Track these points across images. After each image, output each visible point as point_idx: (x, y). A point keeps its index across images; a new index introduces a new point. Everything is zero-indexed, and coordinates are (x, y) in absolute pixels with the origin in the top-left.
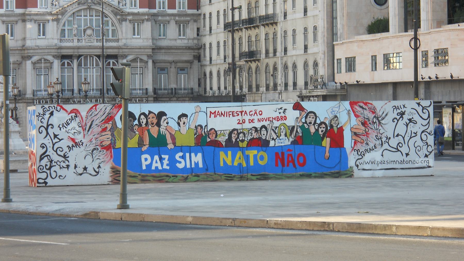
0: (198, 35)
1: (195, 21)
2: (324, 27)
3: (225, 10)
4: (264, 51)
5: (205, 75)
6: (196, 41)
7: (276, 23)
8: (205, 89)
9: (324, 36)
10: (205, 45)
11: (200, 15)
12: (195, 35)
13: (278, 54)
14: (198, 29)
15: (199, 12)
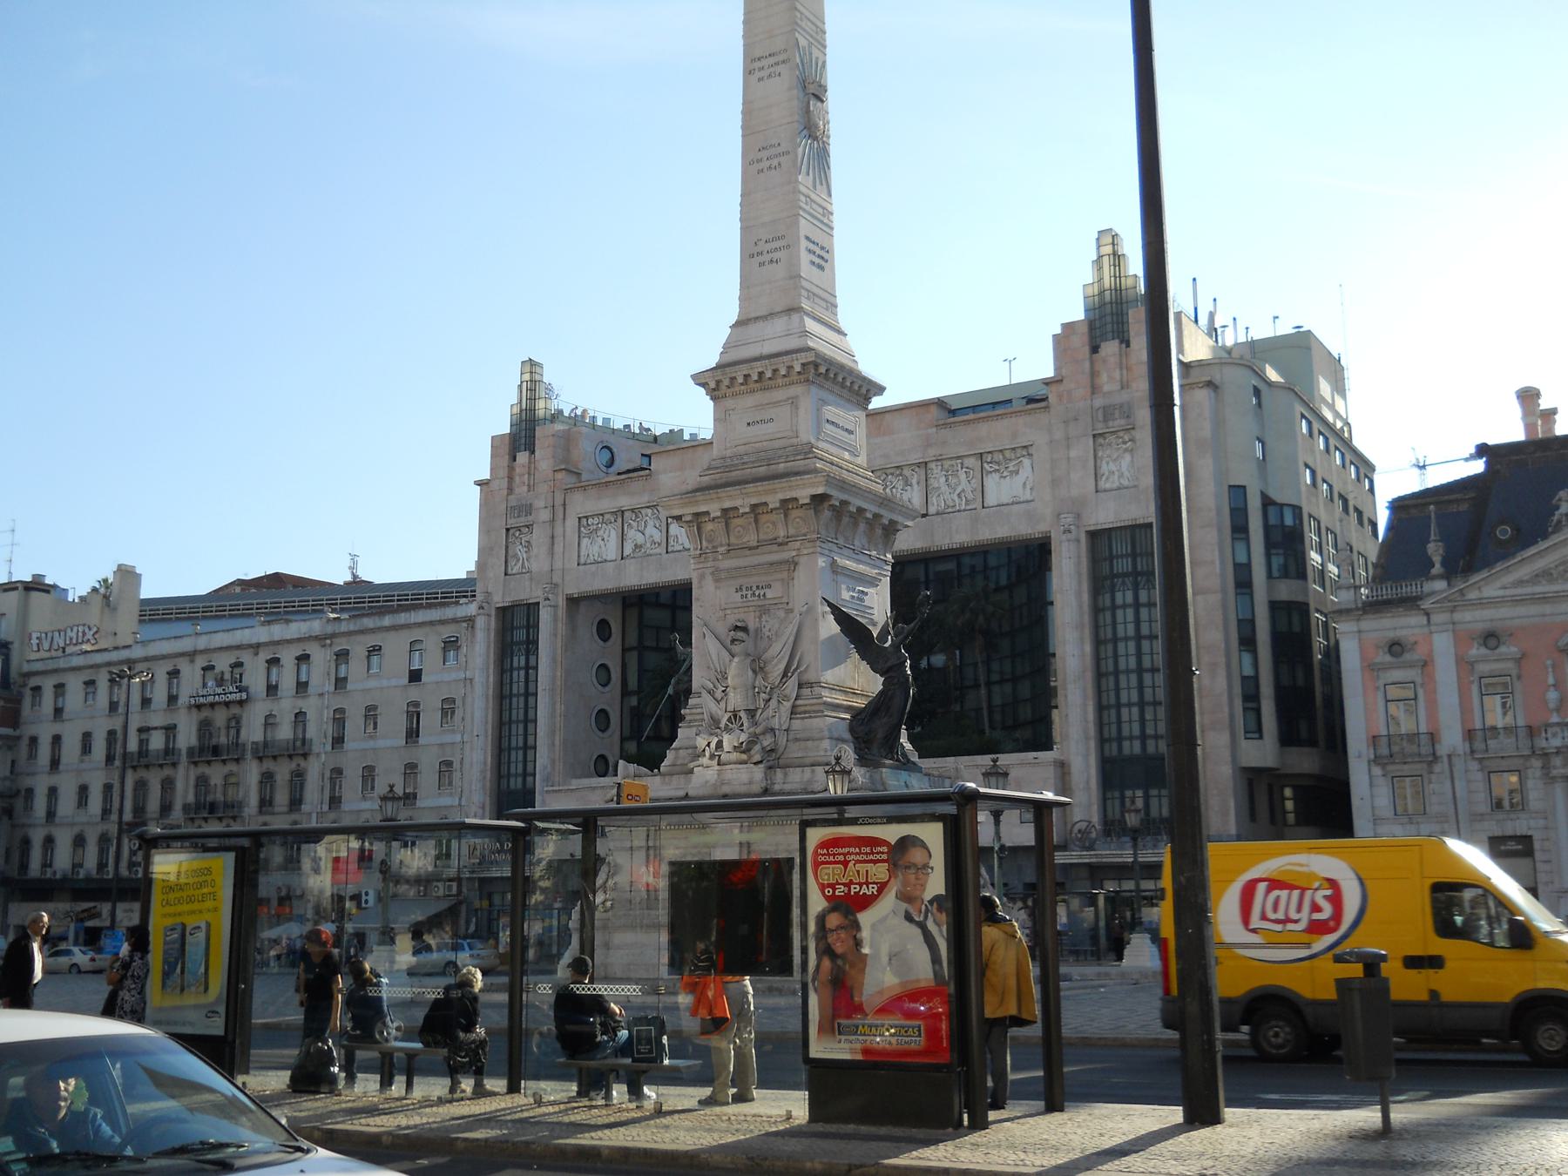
0: (12, 772)
1: (10, 748)
2: (485, 763)
3: (111, 734)
4: (253, 800)
5: (26, 842)
6: (7, 783)
7: (305, 756)
8: (24, 866)
9: (485, 778)
10: (30, 792)
11: (19, 738)
12: (8, 773)
13: (305, 808)
14: (13, 762)
15: (17, 733)
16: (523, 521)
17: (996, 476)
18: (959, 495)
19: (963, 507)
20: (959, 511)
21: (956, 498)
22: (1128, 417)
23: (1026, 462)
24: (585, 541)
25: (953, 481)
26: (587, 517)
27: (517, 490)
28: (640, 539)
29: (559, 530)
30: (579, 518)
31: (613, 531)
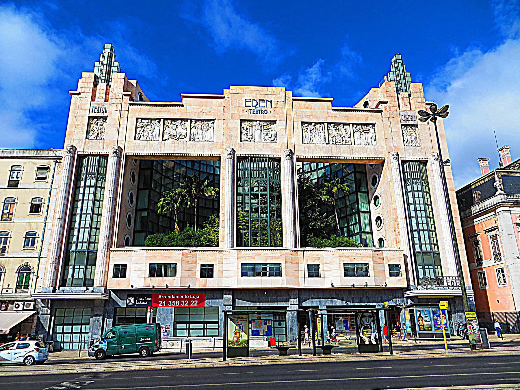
16: (100, 115)
17: (359, 133)
18: (342, 138)
19: (344, 143)
20: (343, 144)
21: (341, 139)
22: (414, 121)
23: (372, 130)
24: (138, 130)
25: (340, 132)
26: (142, 119)
27: (96, 100)
28: (173, 133)
29: (123, 121)
30: (137, 119)
31: (156, 127)
